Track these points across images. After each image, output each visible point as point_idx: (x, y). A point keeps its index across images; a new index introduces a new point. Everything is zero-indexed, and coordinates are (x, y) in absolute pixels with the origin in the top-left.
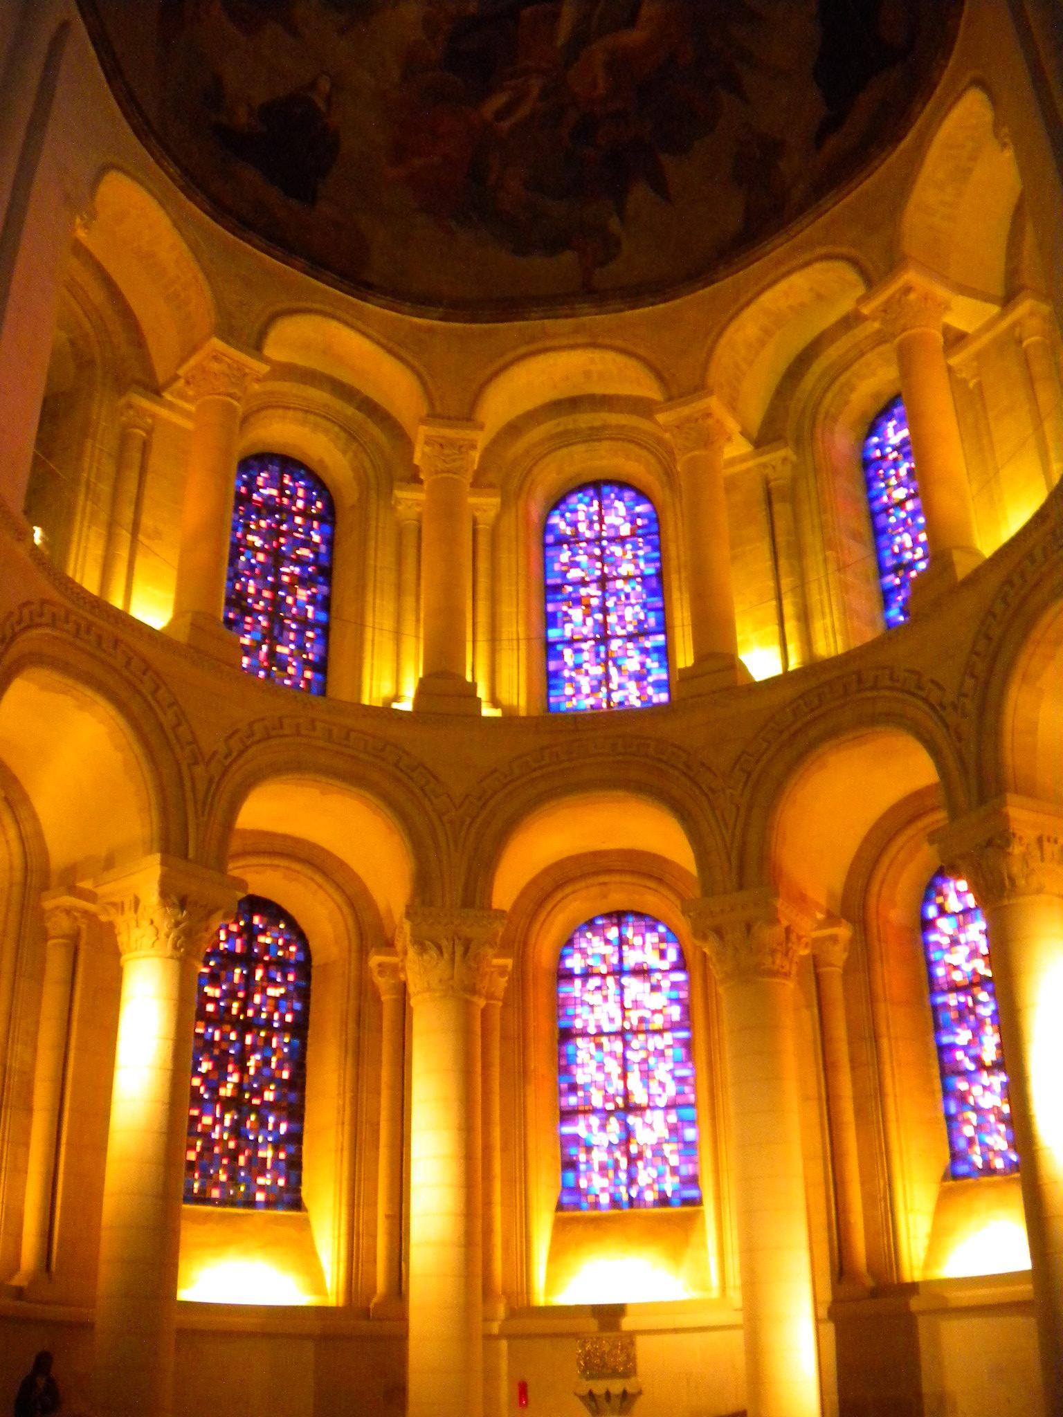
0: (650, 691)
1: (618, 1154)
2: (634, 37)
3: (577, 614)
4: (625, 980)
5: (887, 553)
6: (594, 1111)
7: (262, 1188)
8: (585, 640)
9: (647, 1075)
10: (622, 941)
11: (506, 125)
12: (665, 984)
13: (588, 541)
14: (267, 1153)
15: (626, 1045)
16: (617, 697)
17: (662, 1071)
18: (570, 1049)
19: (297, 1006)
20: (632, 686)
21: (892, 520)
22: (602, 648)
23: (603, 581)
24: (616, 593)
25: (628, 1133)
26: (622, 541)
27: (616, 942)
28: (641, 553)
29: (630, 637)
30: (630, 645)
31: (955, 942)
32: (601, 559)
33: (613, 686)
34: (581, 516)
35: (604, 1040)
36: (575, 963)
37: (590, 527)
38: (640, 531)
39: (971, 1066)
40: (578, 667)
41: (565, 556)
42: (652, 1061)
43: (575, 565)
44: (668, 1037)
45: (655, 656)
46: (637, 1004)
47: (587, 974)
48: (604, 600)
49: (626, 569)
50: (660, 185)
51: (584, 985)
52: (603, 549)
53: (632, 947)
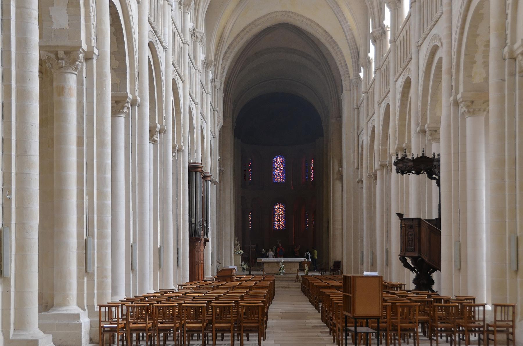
3: (276, 171)
6: (277, 221)
10: (280, 206)
23: (279, 167)
24: (280, 169)
25: (279, 223)
26: (281, 163)
29: (282, 174)
34: (277, 159)
37: (278, 161)
40: (276, 177)
41: (275, 164)
43: (276, 165)
48: (279, 169)
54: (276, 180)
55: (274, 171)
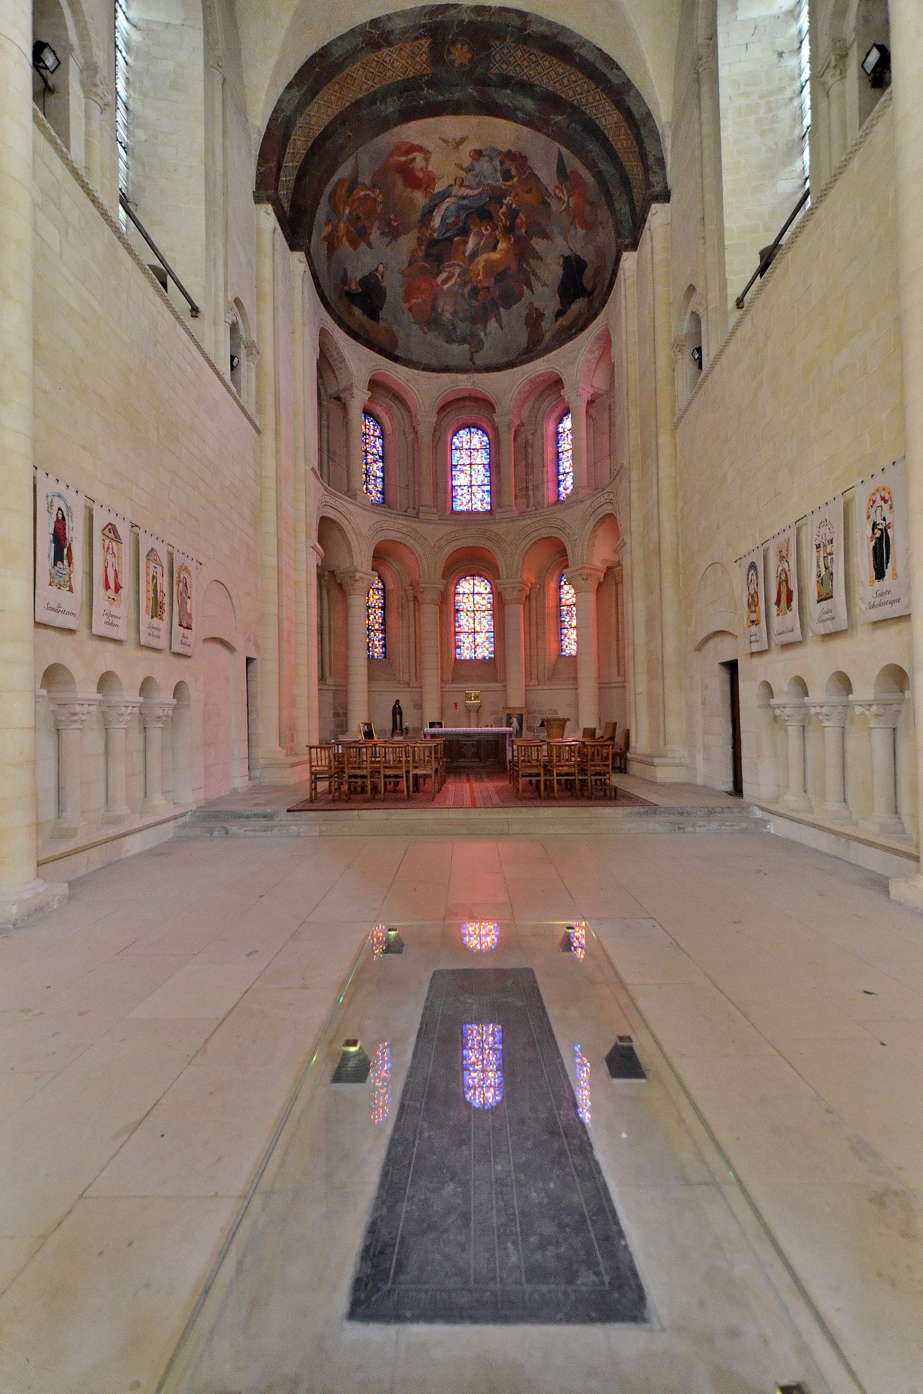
0: (485, 505)
1: (472, 644)
2: (495, 256)
3: (462, 475)
4: (475, 596)
5: (561, 468)
7: (376, 652)
8: (464, 486)
9: (480, 623)
11: (445, 287)
12: (486, 597)
13: (466, 449)
14: (377, 643)
15: (475, 615)
16: (474, 507)
17: (484, 622)
18: (459, 615)
19: (382, 601)
20: (479, 503)
21: (564, 456)
22: (470, 489)
27: (472, 584)
28: (483, 455)
29: (479, 486)
30: (479, 489)
31: (568, 593)
32: (470, 456)
33: (473, 502)
35: (468, 613)
36: (460, 590)
38: (483, 447)
39: (569, 627)
42: (482, 619)
43: (462, 458)
44: (487, 612)
45: (486, 493)
46: (478, 603)
47: (464, 594)
49: (479, 461)
50: (499, 321)
51: (463, 596)
52: (471, 452)
53: (477, 586)
54: (461, 504)
55: (453, 478)
